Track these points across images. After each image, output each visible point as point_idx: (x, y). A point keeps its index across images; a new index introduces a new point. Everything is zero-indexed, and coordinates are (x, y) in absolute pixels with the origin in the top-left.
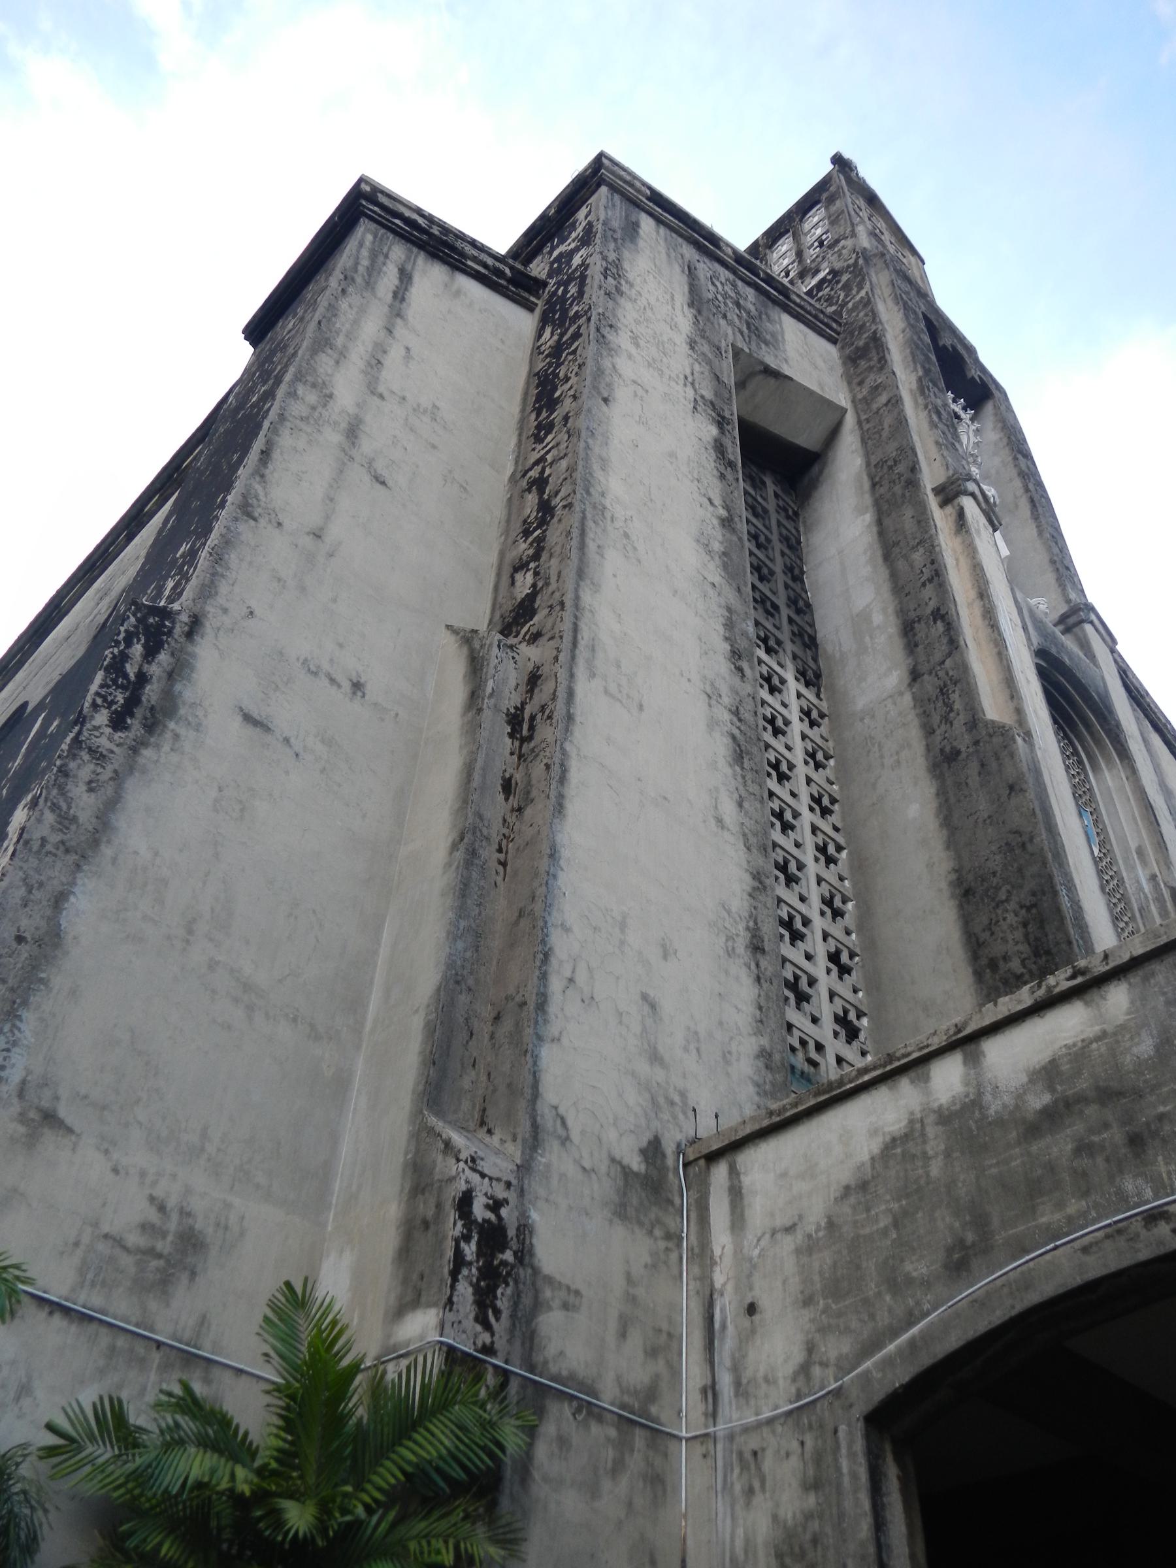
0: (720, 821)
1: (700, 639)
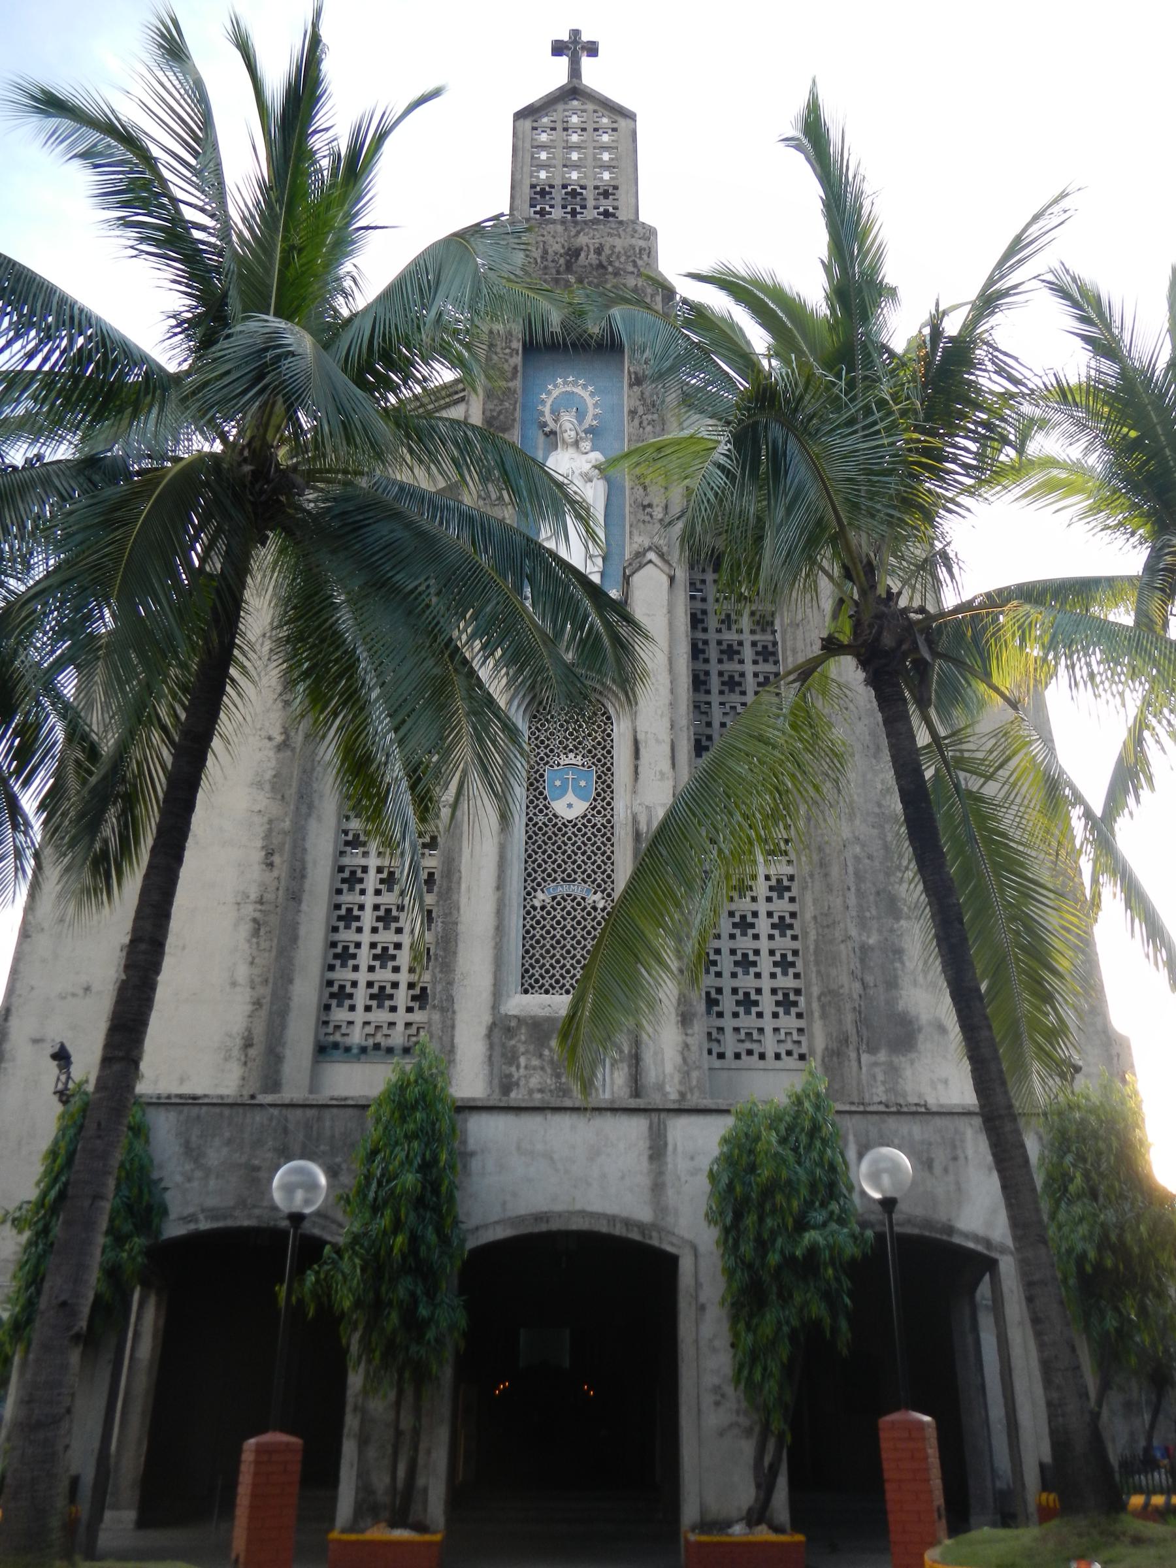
0: (234, 984)
1: (239, 865)
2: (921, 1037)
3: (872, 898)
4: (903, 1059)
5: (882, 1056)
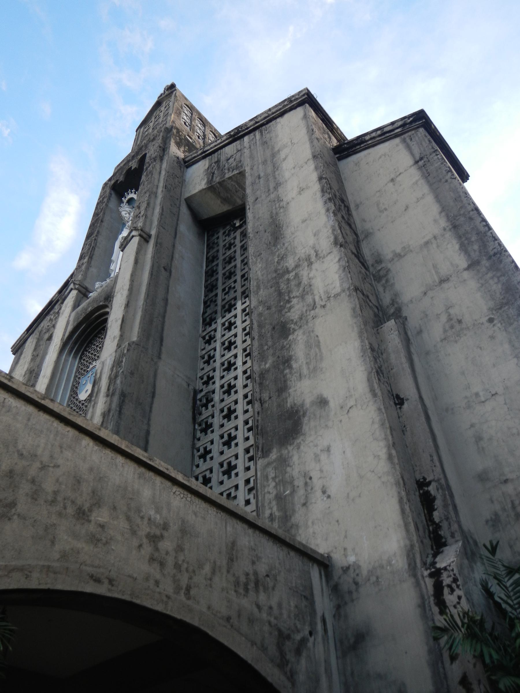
2: (305, 420)
3: (269, 335)
4: (290, 448)
5: (274, 455)
